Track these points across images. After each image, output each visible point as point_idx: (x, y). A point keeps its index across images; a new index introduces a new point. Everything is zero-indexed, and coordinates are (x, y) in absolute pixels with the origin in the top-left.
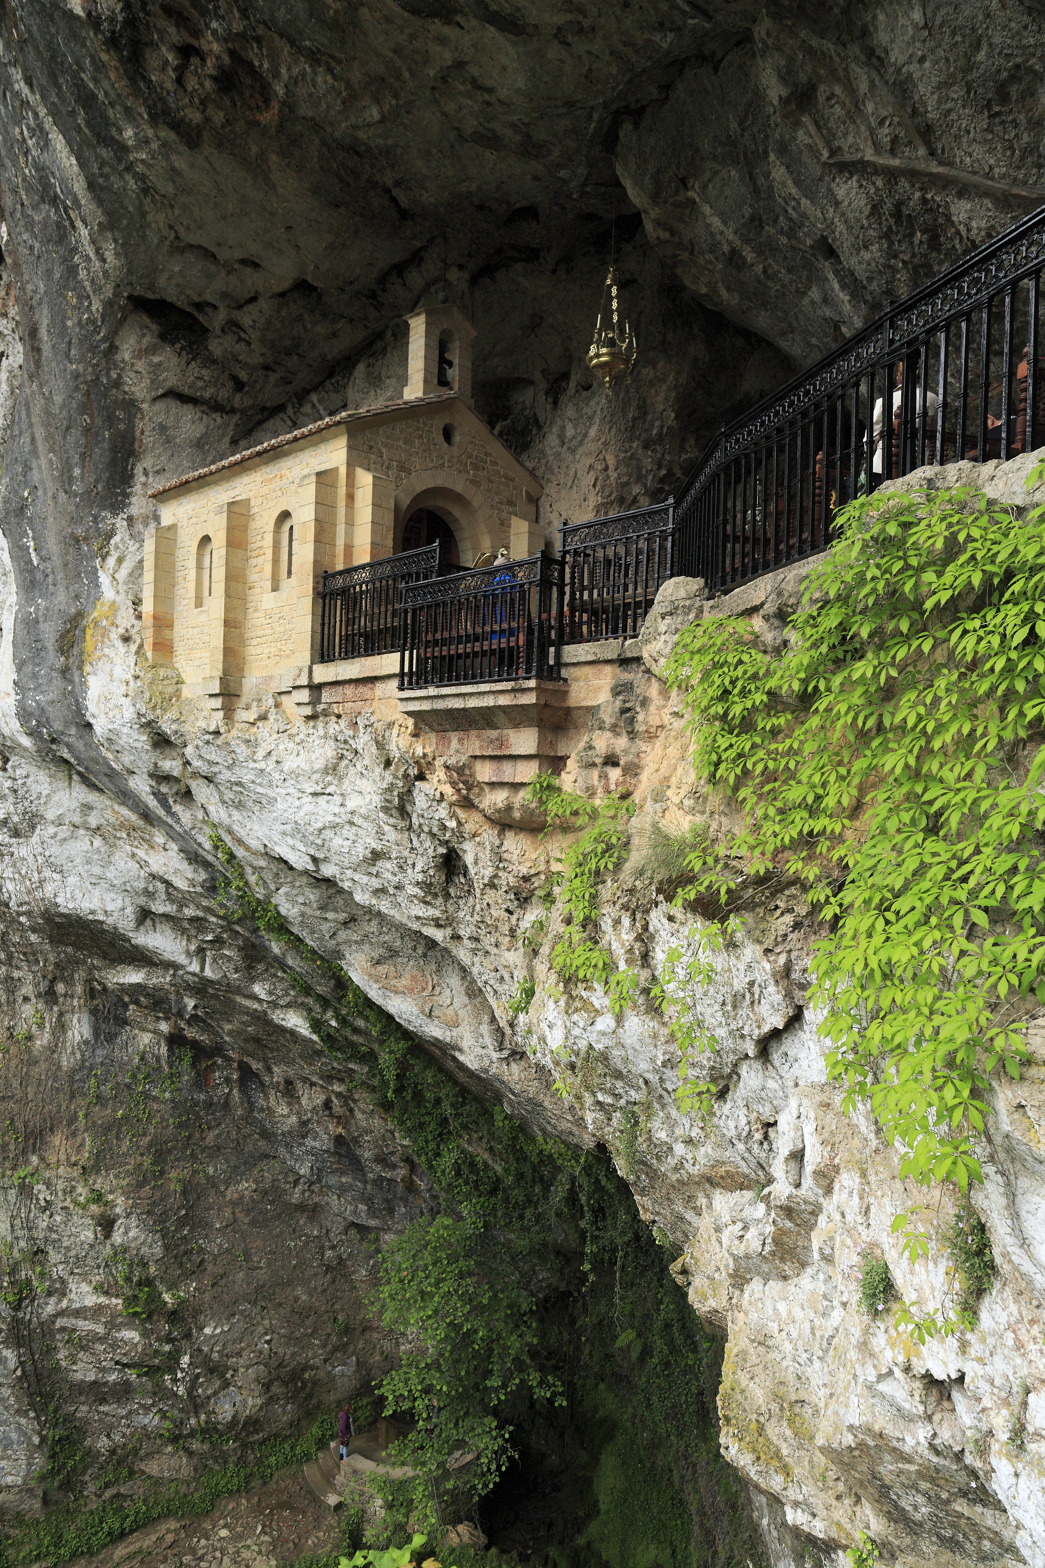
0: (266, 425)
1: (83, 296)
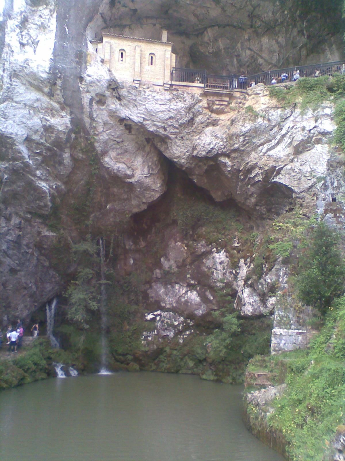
0: (105, 29)
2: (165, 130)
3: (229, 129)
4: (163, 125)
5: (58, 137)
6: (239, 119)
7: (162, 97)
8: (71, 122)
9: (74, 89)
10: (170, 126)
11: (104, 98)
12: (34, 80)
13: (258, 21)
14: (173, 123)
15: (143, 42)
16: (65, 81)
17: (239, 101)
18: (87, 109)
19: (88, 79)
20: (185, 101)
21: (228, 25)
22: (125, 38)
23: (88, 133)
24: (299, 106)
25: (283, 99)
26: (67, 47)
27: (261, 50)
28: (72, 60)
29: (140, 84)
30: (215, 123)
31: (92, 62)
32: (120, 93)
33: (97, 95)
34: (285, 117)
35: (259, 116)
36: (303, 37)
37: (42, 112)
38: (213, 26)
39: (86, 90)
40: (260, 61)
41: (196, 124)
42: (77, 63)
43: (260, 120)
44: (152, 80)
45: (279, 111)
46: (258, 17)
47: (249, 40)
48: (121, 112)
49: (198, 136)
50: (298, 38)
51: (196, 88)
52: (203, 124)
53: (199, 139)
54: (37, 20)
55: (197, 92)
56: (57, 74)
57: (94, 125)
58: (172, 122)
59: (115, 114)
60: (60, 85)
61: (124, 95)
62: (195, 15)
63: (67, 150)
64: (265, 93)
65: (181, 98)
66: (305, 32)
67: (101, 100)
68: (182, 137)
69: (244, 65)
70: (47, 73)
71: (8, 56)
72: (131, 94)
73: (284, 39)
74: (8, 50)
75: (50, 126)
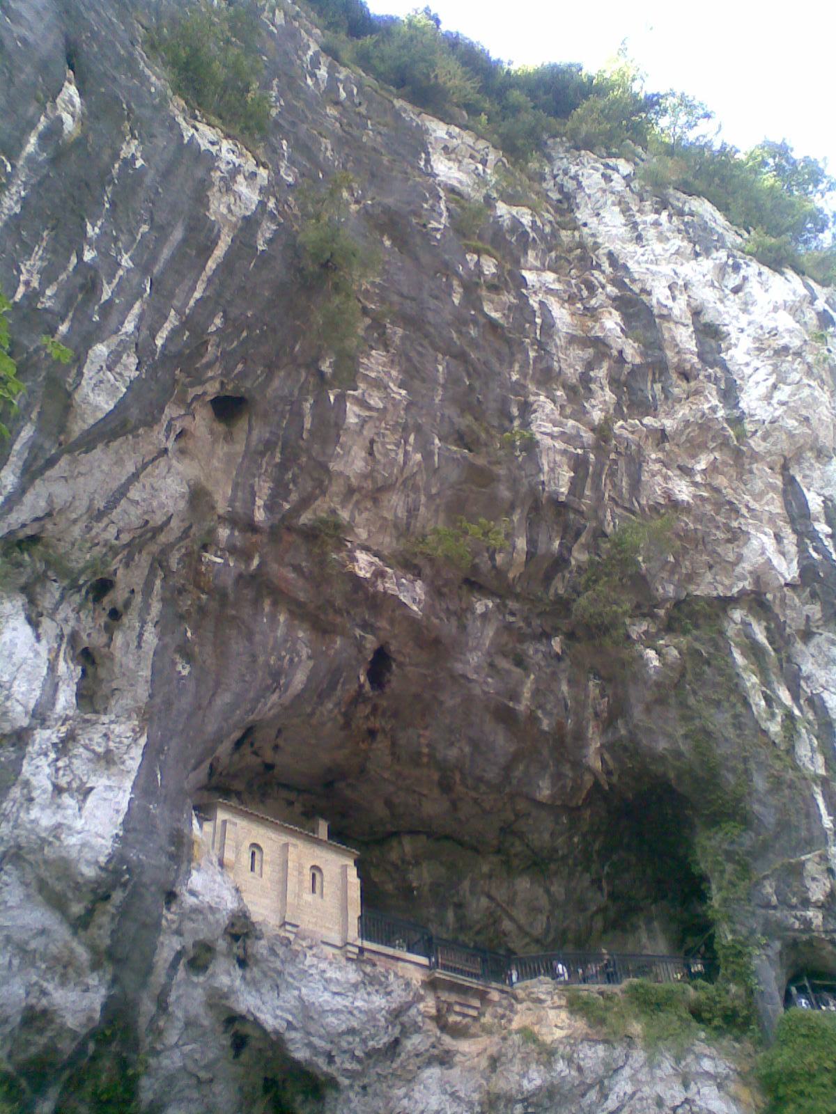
1: (252, 711)
2: (330, 1059)
3: (488, 1079)
4: (328, 1047)
5: (51, 1049)
6: (510, 1055)
7: (336, 975)
8: (105, 1007)
9: (148, 920)
10: (345, 1052)
11: (208, 956)
12: (58, 879)
13: (517, 843)
14: (355, 1045)
15: (298, 838)
16: (135, 894)
17: (500, 1011)
18: (159, 977)
19: (191, 900)
20: (389, 994)
21: (448, 837)
22: (261, 820)
23: (135, 1046)
24: (639, 1042)
25: (602, 1021)
26: (155, 816)
27: (511, 902)
28: (161, 848)
29: (296, 934)
30: (445, 1059)
31: (203, 862)
32: (249, 950)
33: (194, 946)
34: (614, 1066)
35: (557, 1056)
36: (599, 894)
37: (38, 968)
38: (418, 833)
39: (174, 926)
40: (507, 925)
41: (403, 1054)
42: (172, 857)
43: (561, 1065)
44: (317, 929)
45: (601, 1050)
46: (520, 835)
47: (490, 876)
48: (241, 998)
49: (403, 1090)
50: (590, 894)
51: (411, 968)
52: (420, 1059)
53: (406, 1096)
54: (95, 738)
55: (417, 977)
56: (121, 874)
57: (161, 1023)
58: (349, 1043)
59: (224, 1002)
60: (118, 903)
61: (259, 957)
62: (389, 804)
63: (54, 1093)
64: (558, 1002)
65: (381, 984)
66: (604, 885)
67: (198, 959)
68: (364, 1088)
69: (471, 928)
70: (101, 868)
71: (14, 809)
72: (276, 955)
73: (562, 890)
74: (18, 795)
75: (44, 1012)
